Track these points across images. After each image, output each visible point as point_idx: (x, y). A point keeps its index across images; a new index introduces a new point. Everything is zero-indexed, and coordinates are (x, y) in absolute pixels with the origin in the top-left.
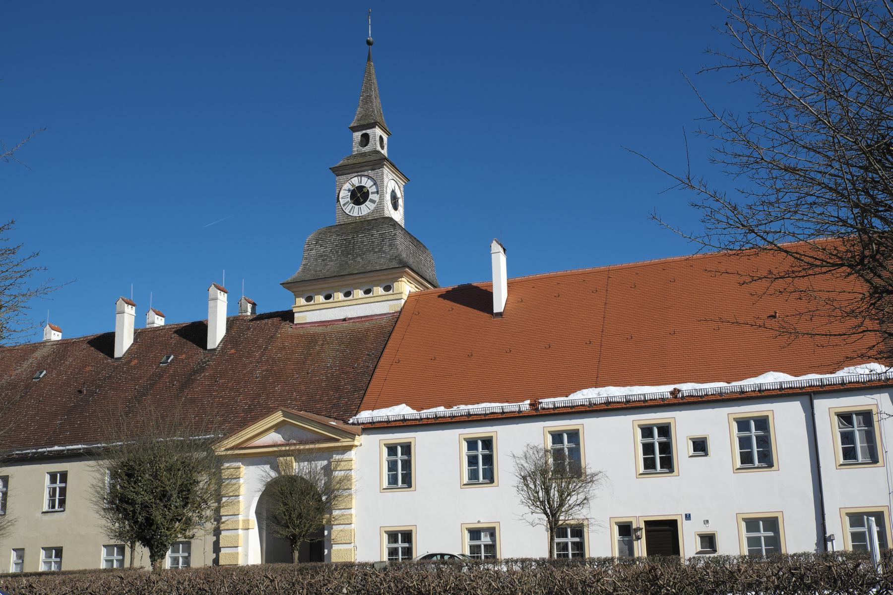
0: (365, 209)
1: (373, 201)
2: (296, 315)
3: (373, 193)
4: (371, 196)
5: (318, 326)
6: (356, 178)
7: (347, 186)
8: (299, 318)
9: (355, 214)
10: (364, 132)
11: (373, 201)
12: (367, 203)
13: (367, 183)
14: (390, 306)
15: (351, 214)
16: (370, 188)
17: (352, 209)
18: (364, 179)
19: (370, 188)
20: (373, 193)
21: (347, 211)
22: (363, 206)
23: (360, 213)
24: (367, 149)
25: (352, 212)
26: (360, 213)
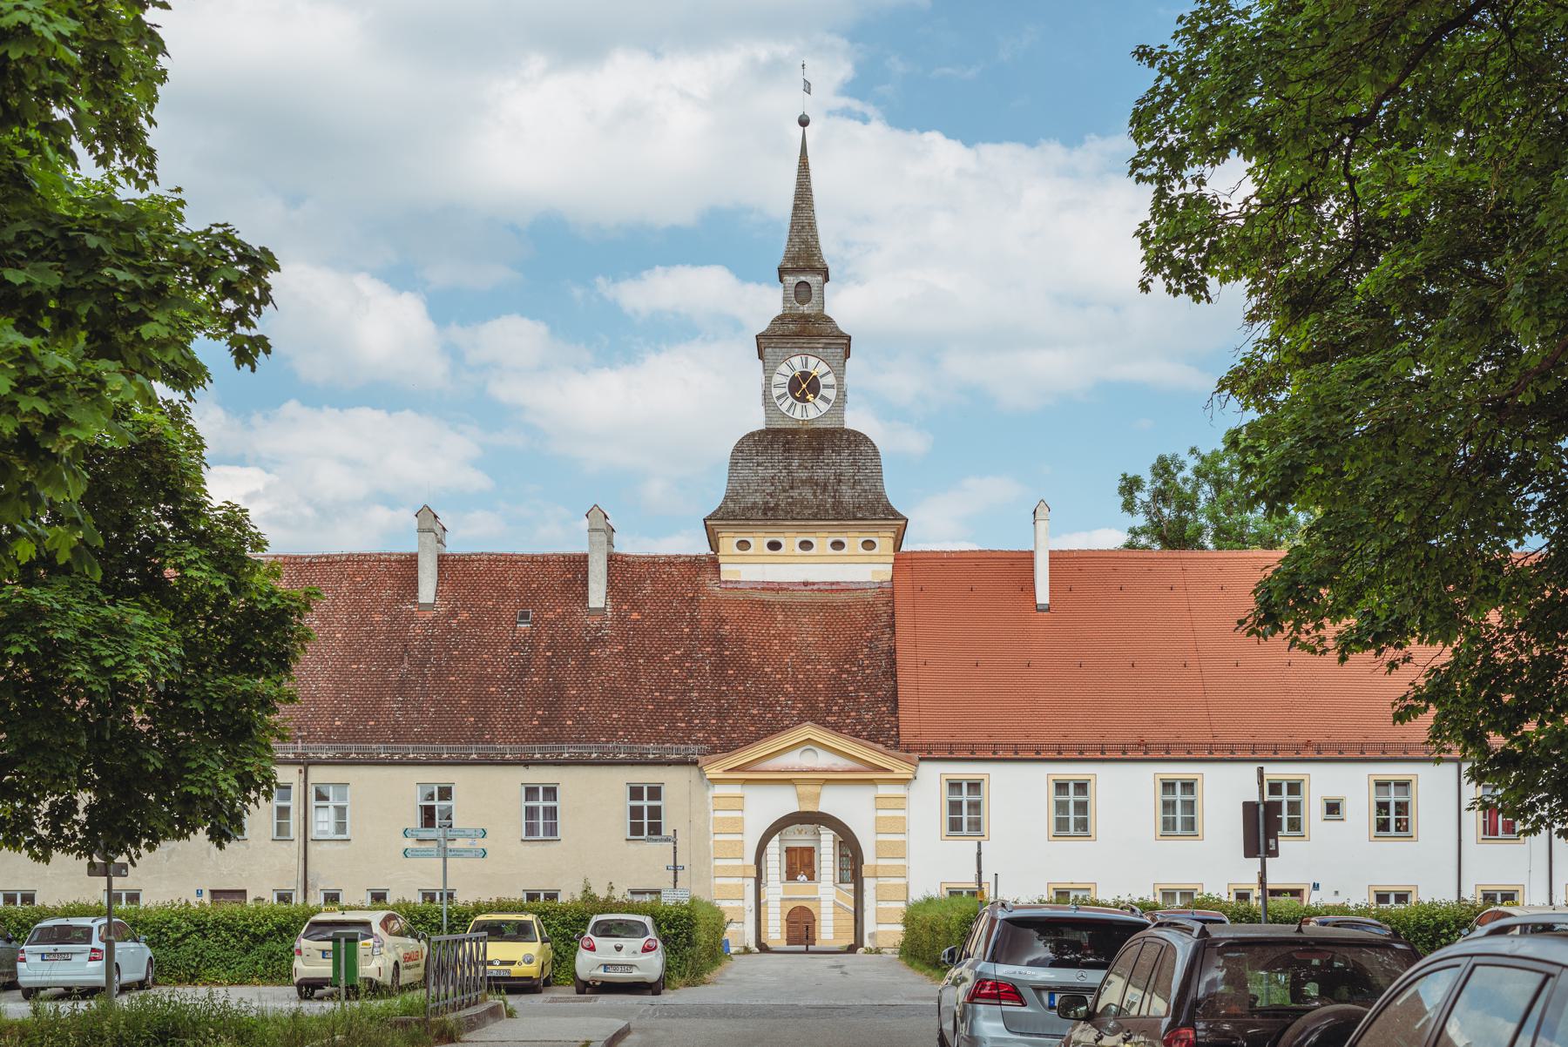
0: (812, 412)
1: (824, 399)
2: (723, 567)
3: (826, 386)
4: (823, 391)
5: (763, 589)
7: (783, 368)
8: (729, 571)
9: (797, 415)
10: (803, 278)
11: (824, 399)
13: (817, 367)
14: (874, 572)
16: (821, 377)
17: (791, 406)
18: (812, 361)
19: (821, 377)
20: (826, 386)
21: (784, 408)
23: (805, 414)
24: (806, 309)
25: (791, 411)
26: (805, 414)
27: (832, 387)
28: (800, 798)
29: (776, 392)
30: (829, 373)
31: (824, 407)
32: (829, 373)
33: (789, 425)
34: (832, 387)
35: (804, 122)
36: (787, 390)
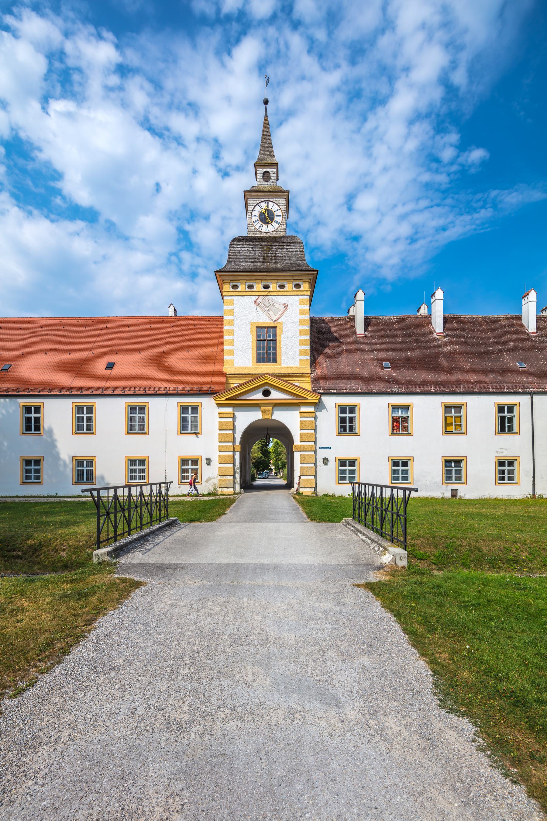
1: (278, 223)
3: (277, 216)
4: (276, 219)
6: (264, 203)
9: (264, 230)
11: (278, 223)
12: (273, 223)
15: (260, 230)
16: (275, 212)
19: (275, 212)
20: (277, 216)
21: (257, 227)
22: (269, 226)
25: (261, 228)
27: (280, 216)
28: (264, 412)
29: (254, 219)
30: (278, 209)
31: (276, 226)
32: (278, 209)
33: (258, 234)
34: (280, 216)
35: (266, 102)
36: (258, 218)
